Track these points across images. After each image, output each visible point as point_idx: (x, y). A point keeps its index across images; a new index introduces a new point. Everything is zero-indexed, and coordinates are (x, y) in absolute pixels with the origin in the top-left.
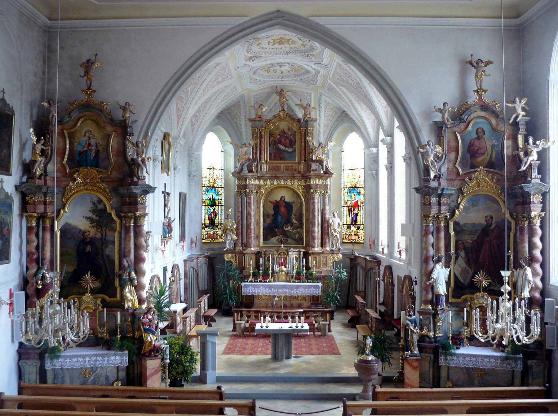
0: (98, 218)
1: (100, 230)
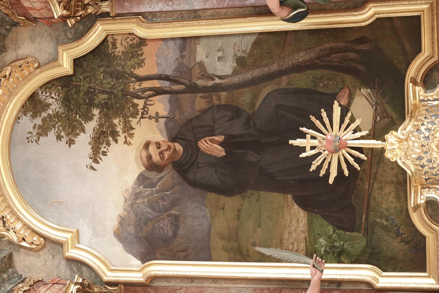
0: (96, 112)
1: (140, 103)
